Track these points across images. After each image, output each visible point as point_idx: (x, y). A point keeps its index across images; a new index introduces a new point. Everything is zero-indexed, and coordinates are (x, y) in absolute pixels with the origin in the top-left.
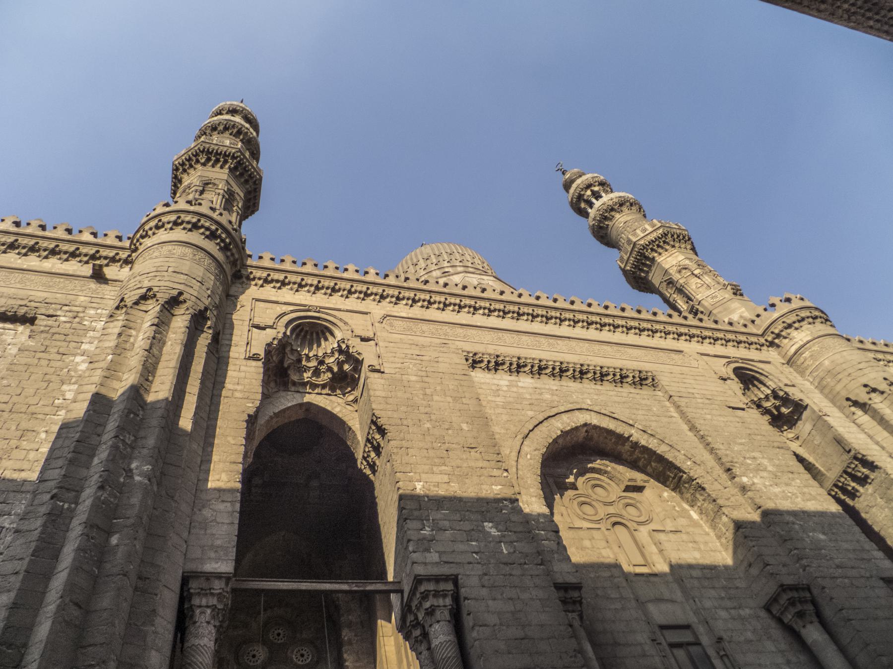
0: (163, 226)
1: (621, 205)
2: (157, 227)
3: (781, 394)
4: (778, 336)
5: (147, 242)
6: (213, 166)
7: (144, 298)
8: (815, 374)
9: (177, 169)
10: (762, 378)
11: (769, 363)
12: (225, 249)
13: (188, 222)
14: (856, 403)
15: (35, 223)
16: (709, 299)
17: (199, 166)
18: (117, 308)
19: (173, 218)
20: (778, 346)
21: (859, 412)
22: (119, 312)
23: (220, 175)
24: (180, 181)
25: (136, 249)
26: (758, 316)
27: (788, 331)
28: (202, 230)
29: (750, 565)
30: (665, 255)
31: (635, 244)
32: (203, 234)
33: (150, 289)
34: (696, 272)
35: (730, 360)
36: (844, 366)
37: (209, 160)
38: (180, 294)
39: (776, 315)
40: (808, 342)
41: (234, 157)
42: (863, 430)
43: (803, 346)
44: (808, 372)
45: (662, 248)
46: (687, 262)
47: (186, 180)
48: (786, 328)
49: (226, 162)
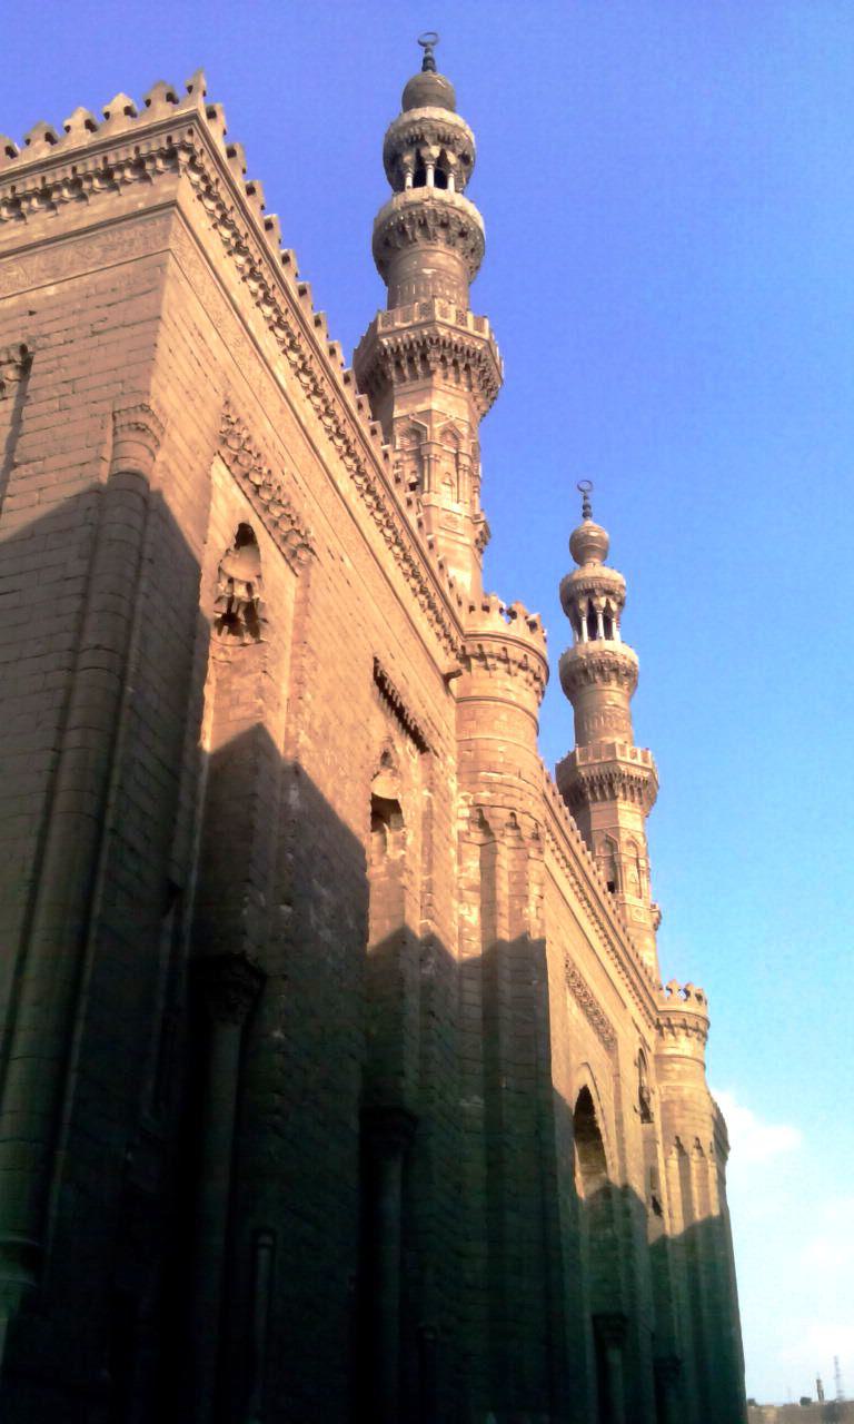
1: (627, 675)
3: (645, 1095)
4: (670, 1026)
8: (670, 1092)
10: (643, 1069)
11: (649, 1050)
14: (680, 1147)
16: (634, 909)
20: (662, 1034)
21: (675, 1155)
26: (671, 990)
27: (682, 1031)
29: (605, 1280)
30: (628, 802)
31: (615, 761)
34: (642, 863)
35: (643, 1041)
36: (696, 1107)
39: (685, 1007)
40: (686, 1057)
42: (667, 1172)
43: (680, 1057)
44: (665, 1083)
45: (633, 793)
46: (641, 839)
48: (682, 1027)
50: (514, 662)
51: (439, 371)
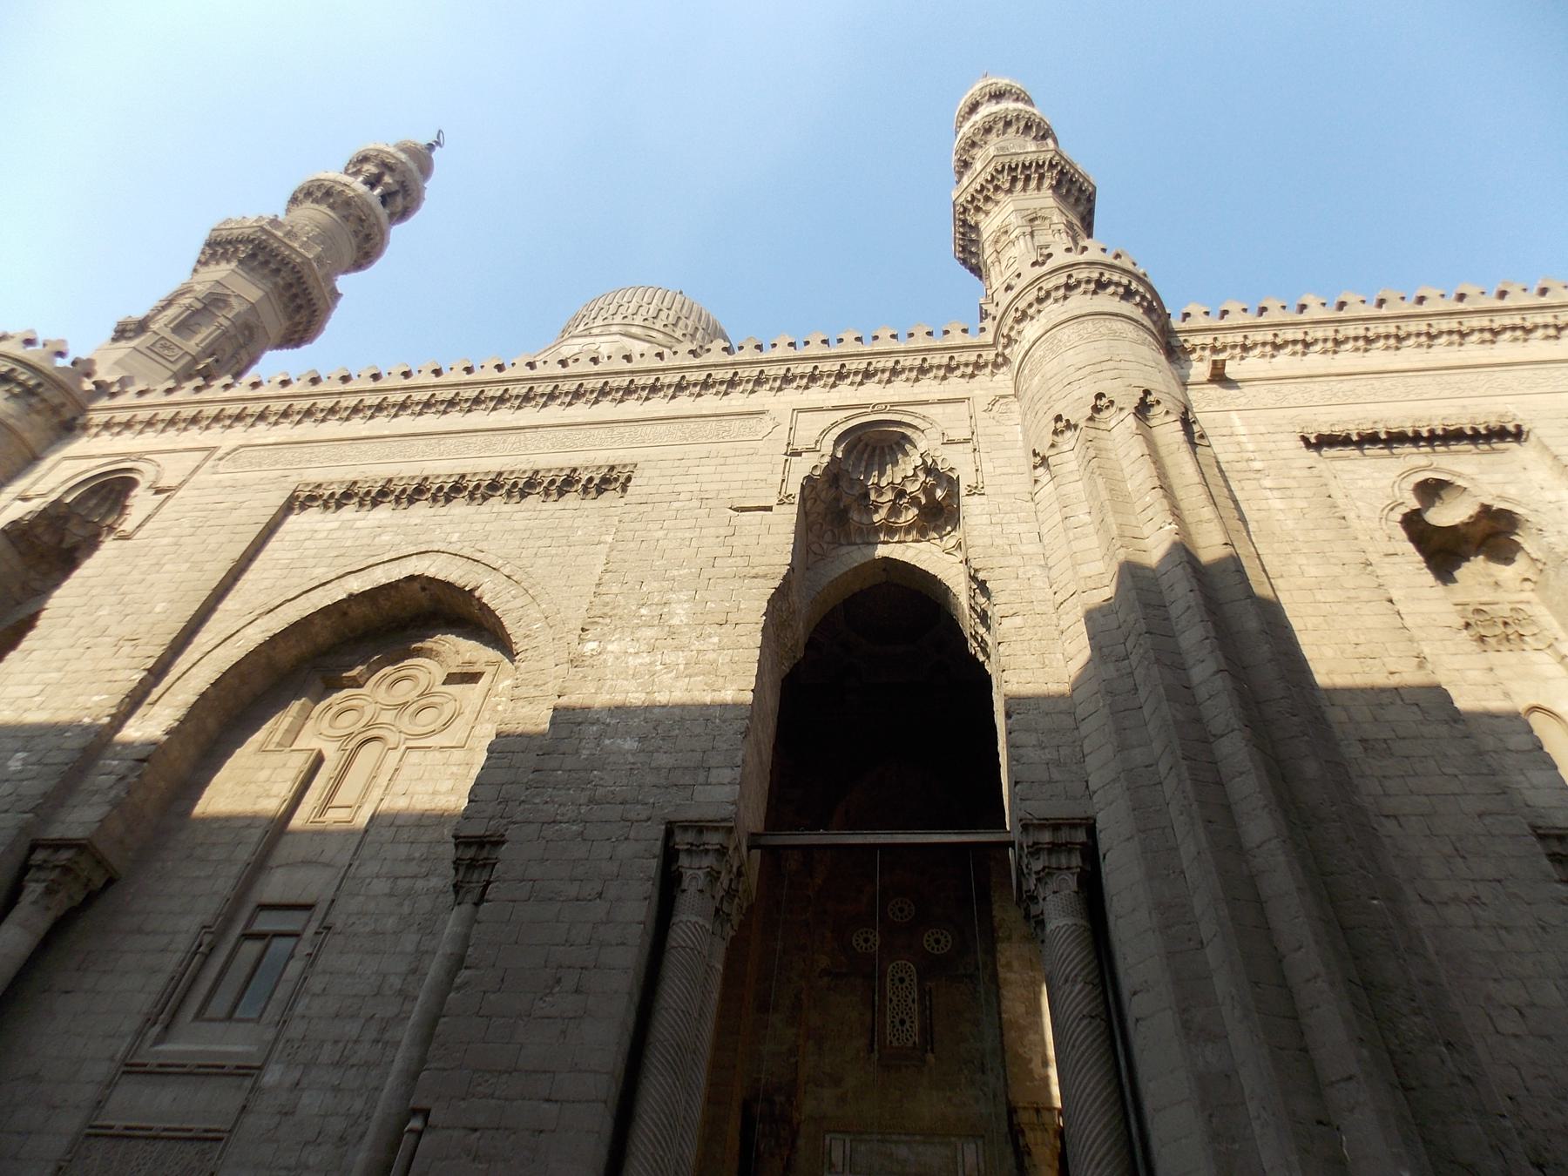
0: (1048, 294)
2: (1040, 300)
5: (1031, 330)
6: (1024, 189)
7: (1097, 409)
9: (965, 210)
12: (1149, 311)
13: (1088, 282)
15: (849, 337)
17: (1000, 196)
18: (1055, 432)
19: (1062, 279)
22: (1059, 439)
23: (1043, 199)
24: (975, 228)
25: (1010, 341)
28: (1112, 289)
32: (1114, 294)
33: (1100, 396)
37: (1014, 180)
38: (1147, 392)
41: (1052, 166)
47: (989, 225)
49: (1042, 177)
50: (1030, 305)
51: (981, 216)
